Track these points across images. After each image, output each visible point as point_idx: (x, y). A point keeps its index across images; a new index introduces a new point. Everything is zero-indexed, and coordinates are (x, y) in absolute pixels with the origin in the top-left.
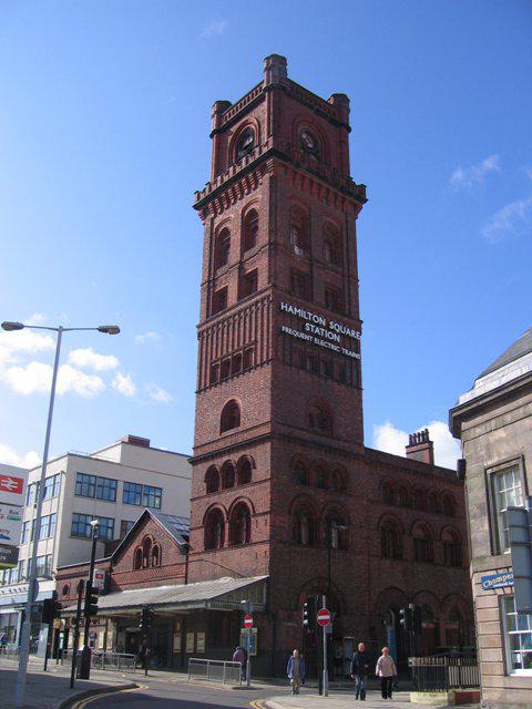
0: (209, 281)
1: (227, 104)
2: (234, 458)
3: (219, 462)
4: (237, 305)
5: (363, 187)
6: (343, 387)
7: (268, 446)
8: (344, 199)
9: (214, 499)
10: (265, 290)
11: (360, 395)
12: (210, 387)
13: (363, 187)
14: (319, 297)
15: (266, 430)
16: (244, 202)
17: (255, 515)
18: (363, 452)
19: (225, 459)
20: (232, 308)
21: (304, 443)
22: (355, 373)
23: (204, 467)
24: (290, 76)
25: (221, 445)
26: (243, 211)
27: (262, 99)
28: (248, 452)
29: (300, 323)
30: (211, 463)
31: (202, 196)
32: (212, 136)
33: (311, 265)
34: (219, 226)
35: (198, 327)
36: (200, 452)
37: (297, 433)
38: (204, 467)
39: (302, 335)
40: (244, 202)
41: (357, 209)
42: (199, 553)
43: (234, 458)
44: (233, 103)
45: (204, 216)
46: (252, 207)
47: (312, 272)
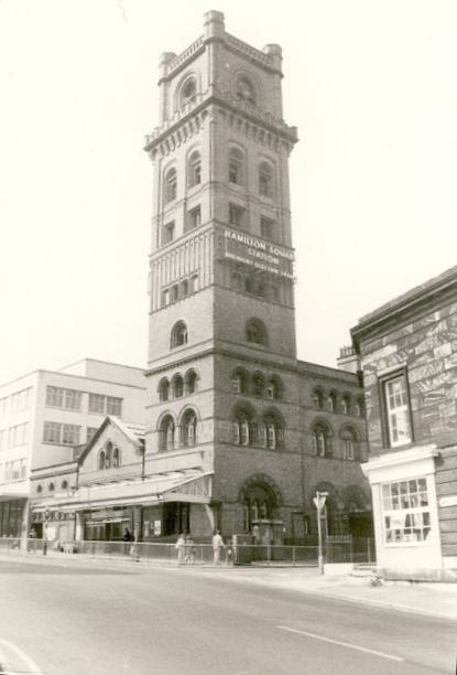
0: (158, 216)
1: (173, 55)
2: (183, 371)
3: (169, 375)
5: (294, 128)
6: (277, 308)
7: (211, 360)
8: (277, 140)
9: (165, 406)
11: (293, 314)
13: (294, 128)
14: (255, 227)
15: (210, 346)
17: (201, 420)
18: (295, 364)
20: (179, 240)
21: (242, 358)
22: (288, 294)
23: (156, 380)
24: (226, 30)
27: (202, 51)
28: (194, 365)
31: (151, 140)
32: (159, 84)
33: (248, 200)
34: (166, 168)
37: (236, 349)
38: (156, 380)
41: (289, 148)
42: (153, 454)
44: (178, 54)
46: (193, 151)
47: (248, 205)
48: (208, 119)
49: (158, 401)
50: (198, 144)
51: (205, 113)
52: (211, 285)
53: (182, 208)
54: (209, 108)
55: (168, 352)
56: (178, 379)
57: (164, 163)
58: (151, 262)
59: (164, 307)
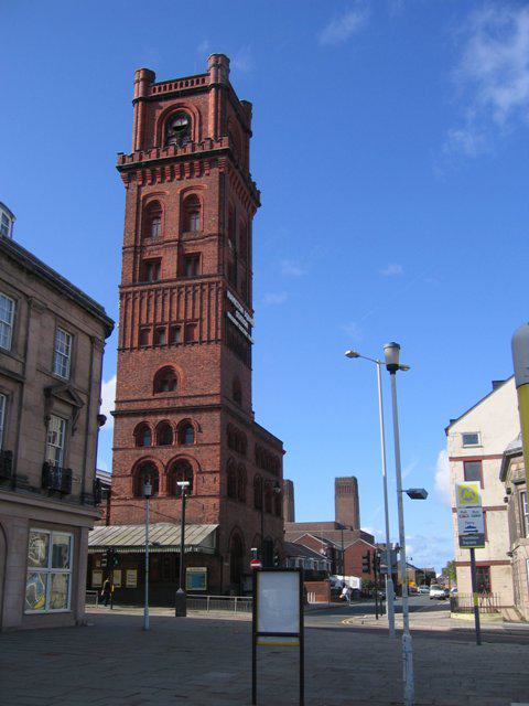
2: (175, 420)
4: (176, 280)
7: (217, 415)
9: (143, 452)
15: (216, 401)
25: (155, 405)
28: (190, 416)
29: (233, 310)
30: (141, 419)
36: (124, 407)
39: (234, 321)
40: (185, 183)
41: (254, 211)
43: (175, 420)
45: (128, 180)
46: (193, 192)
48: (215, 172)
50: (199, 187)
54: (222, 159)
55: (150, 396)
56: (164, 429)
58: (122, 295)
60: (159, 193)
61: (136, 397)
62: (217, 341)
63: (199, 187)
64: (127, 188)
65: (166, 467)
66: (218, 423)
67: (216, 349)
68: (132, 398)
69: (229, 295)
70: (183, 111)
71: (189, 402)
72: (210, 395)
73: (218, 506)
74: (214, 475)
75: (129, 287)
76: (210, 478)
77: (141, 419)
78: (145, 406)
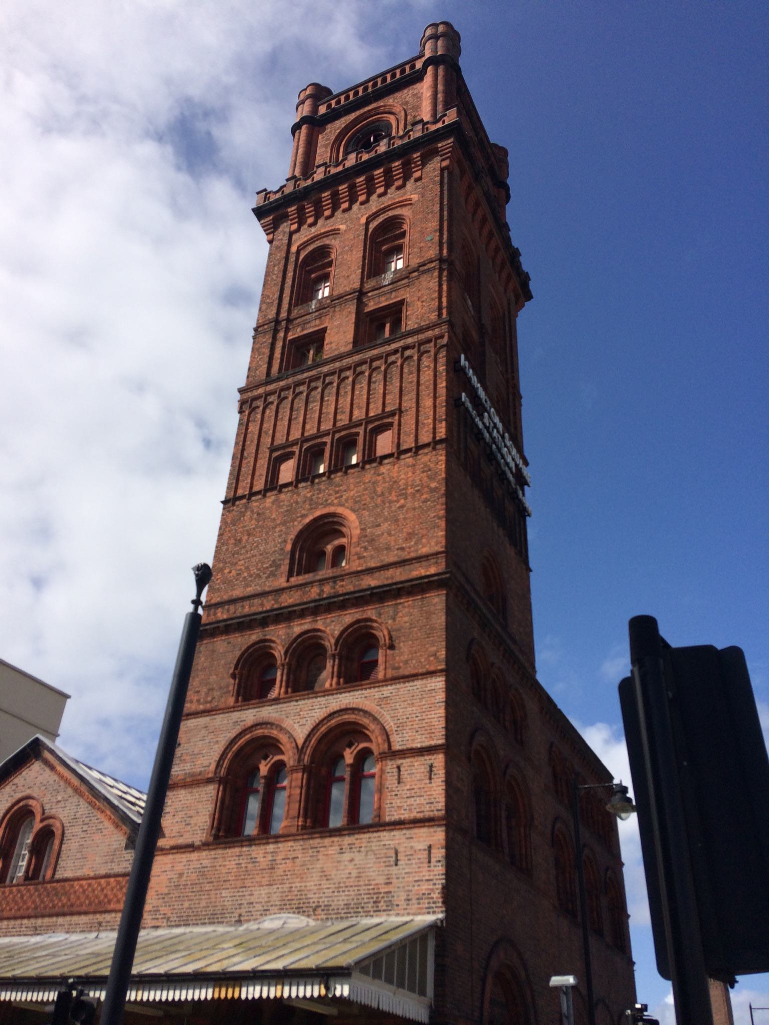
0: (277, 321)
4: (349, 354)
9: (249, 716)
10: (428, 328)
12: (264, 493)
16: (375, 204)
17: (392, 754)
19: (298, 627)
25: (288, 599)
26: (367, 224)
27: (418, 77)
28: (370, 612)
30: (254, 636)
34: (298, 252)
35: (241, 391)
40: (375, 204)
42: (190, 848)
45: (271, 229)
48: (435, 165)
49: (231, 701)
51: (435, 152)
52: (435, 443)
53: (352, 308)
54: (446, 144)
55: (282, 582)
57: (299, 239)
58: (242, 403)
59: (273, 485)
60: (327, 234)
61: (250, 590)
62: (435, 443)
63: (403, 204)
64: (270, 242)
65: (300, 751)
66: (440, 620)
67: (437, 461)
68: (238, 592)
69: (463, 361)
70: (378, 120)
71: (371, 581)
72: (419, 559)
73: (439, 853)
74: (427, 759)
75: (258, 386)
76: (415, 768)
77: (254, 636)
78: (269, 604)
